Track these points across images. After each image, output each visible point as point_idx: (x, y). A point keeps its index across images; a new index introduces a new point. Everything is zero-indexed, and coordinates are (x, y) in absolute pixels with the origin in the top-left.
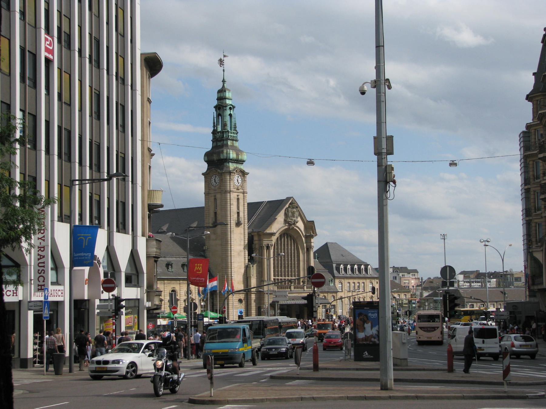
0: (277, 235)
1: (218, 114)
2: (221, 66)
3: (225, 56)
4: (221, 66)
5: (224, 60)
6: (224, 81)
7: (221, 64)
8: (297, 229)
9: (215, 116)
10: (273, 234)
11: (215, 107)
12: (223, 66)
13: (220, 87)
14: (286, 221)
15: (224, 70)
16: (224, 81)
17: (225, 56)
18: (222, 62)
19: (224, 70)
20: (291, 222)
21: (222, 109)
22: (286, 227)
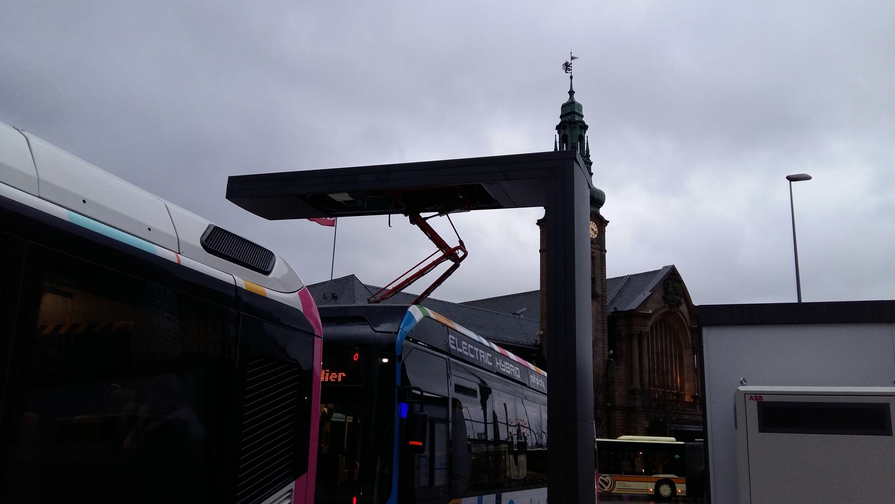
0: (653, 319)
1: (561, 135)
2: (567, 72)
3: (572, 58)
4: (568, 71)
5: (571, 64)
6: (571, 93)
7: (566, 69)
8: (680, 315)
9: (558, 141)
10: (648, 316)
11: (558, 128)
12: (570, 71)
13: (566, 99)
14: (665, 299)
15: (571, 78)
16: (571, 93)
17: (572, 58)
18: (569, 66)
19: (571, 78)
20: (673, 302)
21: (568, 129)
22: (666, 310)
